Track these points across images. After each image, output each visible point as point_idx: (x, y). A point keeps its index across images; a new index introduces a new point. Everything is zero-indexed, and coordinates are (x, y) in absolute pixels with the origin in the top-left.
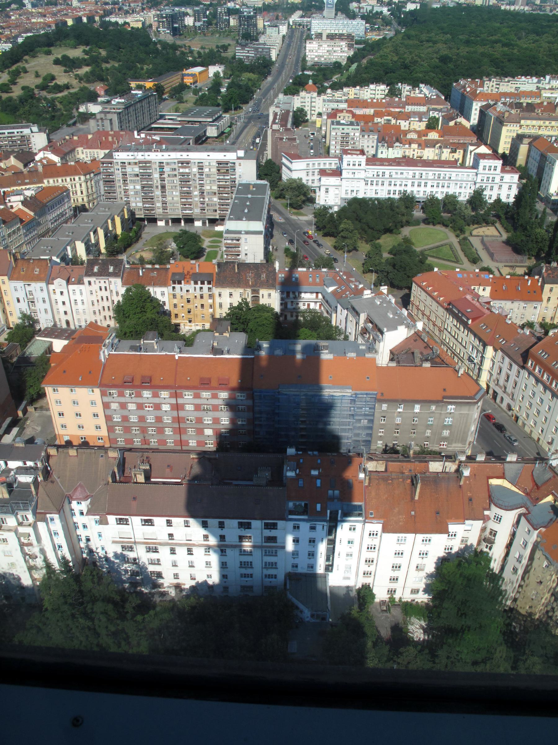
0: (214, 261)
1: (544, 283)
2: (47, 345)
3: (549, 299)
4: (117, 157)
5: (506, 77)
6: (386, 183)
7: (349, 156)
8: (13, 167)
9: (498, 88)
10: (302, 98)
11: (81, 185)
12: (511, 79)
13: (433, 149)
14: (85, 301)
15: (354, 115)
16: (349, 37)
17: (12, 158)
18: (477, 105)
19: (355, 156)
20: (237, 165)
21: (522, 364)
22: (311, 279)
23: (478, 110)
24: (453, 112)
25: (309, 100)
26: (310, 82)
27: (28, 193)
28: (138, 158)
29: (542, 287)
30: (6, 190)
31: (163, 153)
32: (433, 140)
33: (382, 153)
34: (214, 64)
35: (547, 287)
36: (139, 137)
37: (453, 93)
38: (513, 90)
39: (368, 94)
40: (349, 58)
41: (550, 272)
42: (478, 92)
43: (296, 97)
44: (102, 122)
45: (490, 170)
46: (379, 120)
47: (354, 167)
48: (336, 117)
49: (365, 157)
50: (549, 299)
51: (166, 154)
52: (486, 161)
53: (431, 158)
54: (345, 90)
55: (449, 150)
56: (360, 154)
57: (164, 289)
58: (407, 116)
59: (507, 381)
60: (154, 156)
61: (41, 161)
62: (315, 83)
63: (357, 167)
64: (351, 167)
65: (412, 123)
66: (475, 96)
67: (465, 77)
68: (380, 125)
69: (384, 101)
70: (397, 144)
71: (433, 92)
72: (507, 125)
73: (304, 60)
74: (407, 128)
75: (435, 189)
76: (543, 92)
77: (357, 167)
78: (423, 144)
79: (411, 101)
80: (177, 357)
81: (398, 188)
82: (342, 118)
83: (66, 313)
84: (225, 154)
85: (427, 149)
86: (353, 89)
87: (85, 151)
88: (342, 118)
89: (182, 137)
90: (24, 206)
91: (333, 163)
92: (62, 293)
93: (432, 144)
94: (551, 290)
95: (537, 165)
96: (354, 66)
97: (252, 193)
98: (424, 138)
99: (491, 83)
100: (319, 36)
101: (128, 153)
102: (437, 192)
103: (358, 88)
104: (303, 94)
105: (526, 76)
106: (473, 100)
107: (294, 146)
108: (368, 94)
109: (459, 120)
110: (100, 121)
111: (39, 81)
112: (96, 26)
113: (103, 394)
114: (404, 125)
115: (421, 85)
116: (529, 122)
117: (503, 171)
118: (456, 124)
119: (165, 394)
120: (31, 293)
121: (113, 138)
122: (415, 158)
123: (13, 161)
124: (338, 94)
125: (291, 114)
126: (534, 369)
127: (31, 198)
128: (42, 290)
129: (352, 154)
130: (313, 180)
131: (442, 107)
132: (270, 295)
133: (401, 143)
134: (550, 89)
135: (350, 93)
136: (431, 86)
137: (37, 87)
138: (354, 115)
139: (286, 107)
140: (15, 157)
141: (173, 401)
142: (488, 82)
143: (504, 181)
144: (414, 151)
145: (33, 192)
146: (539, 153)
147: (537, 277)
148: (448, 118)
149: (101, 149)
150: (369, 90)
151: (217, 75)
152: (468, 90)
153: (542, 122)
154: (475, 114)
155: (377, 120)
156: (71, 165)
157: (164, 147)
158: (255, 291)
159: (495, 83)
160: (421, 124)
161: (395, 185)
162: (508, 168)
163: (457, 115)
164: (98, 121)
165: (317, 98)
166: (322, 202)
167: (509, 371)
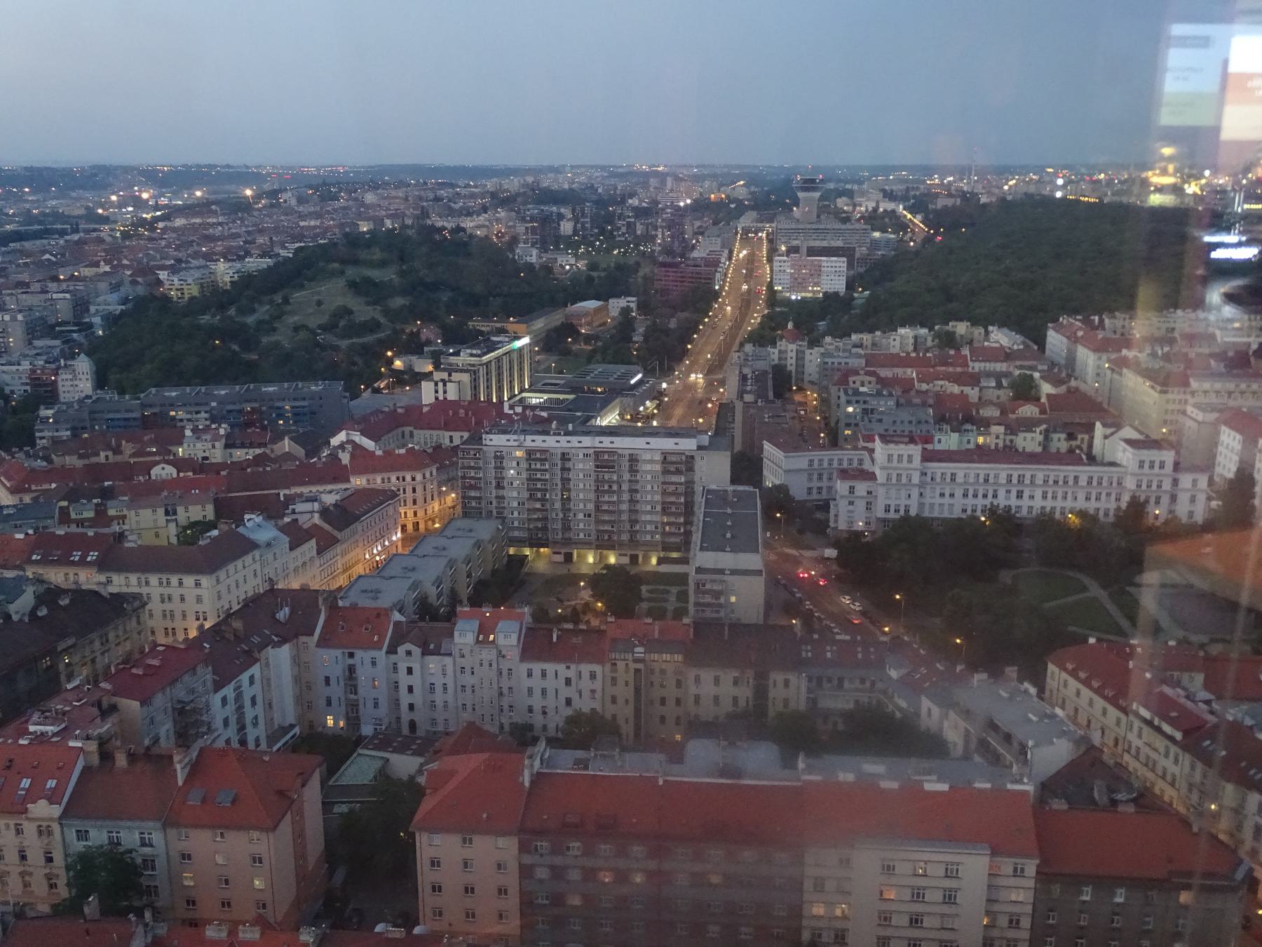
0: (686, 620)
2: (379, 764)
4: (488, 443)
6: (959, 493)
8: (288, 456)
11: (414, 490)
14: (448, 686)
17: (287, 440)
19: (902, 446)
20: (697, 458)
22: (860, 656)
25: (794, 354)
27: (330, 499)
28: (526, 444)
30: (287, 492)
31: (569, 438)
34: (618, 295)
36: (511, 412)
44: (445, 385)
45: (1152, 467)
46: (924, 387)
51: (574, 439)
54: (854, 337)
55: (1063, 436)
57: (597, 668)
60: (550, 442)
61: (342, 446)
68: (931, 394)
70: (968, 427)
75: (1049, 504)
80: (661, 782)
81: (980, 502)
82: (858, 383)
83: (411, 707)
84: (676, 440)
85: (1022, 435)
87: (416, 432)
88: (858, 383)
89: (579, 414)
90: (325, 520)
92: (410, 671)
97: (732, 505)
101: (508, 437)
102: (1053, 508)
103: (878, 333)
104: (782, 345)
110: (440, 384)
111: (324, 320)
112: (410, 232)
113: (524, 848)
114: (972, 393)
119: (637, 850)
120: (352, 669)
121: (467, 414)
123: (286, 445)
125: (771, 376)
127: (336, 505)
128: (374, 664)
129: (897, 443)
130: (820, 488)
132: (787, 683)
137: (320, 327)
138: (881, 381)
139: (762, 365)
140: (291, 439)
141: (652, 865)
144: (997, 437)
145: (338, 497)
149: (446, 430)
151: (626, 311)
156: (399, 455)
157: (570, 426)
158: (761, 677)
160: (1001, 392)
161: (975, 496)
164: (436, 384)
165: (808, 352)
166: (842, 526)
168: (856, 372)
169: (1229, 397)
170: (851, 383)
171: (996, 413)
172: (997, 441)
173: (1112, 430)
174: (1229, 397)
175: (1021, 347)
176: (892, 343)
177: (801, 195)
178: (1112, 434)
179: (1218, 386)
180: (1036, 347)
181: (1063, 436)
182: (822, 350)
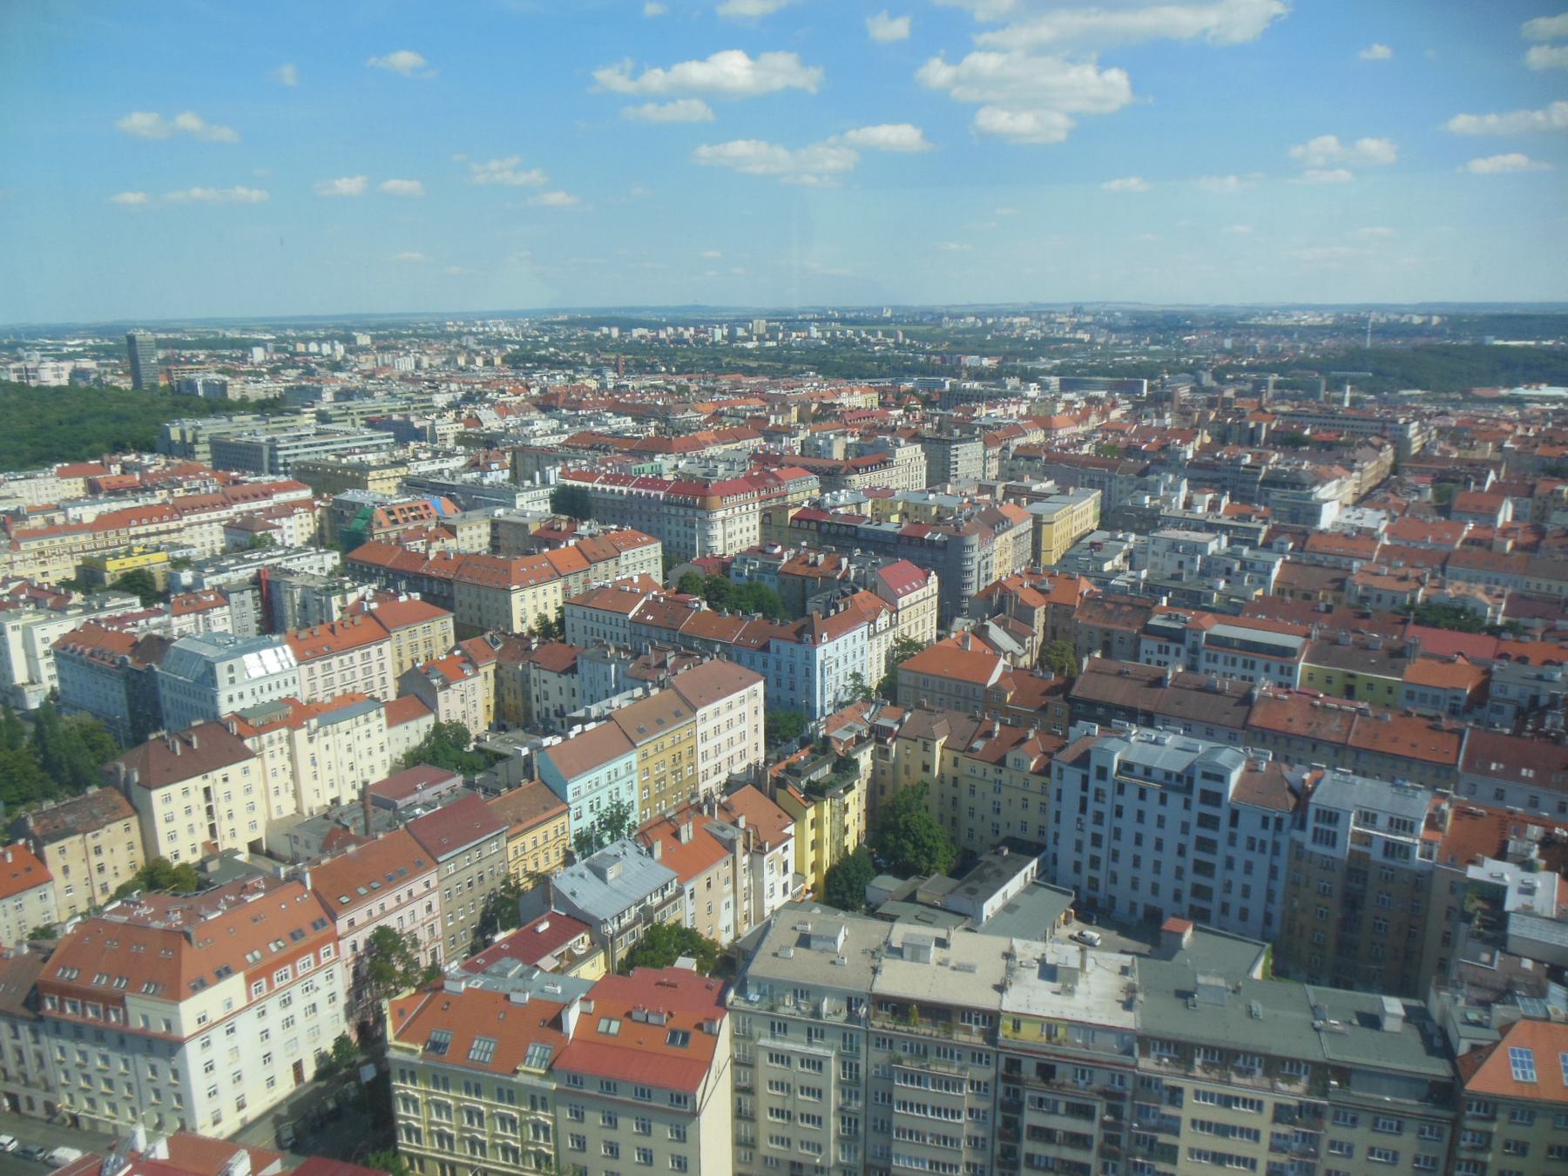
1: (39, 845)
3: (66, 870)
21: (33, 1016)
29: (40, 857)
35: (50, 850)
41: (44, 822)
50: (66, 870)
59: (21, 1061)
94: (62, 851)
126: (62, 1010)
147: (21, 842)
167: (16, 1042)
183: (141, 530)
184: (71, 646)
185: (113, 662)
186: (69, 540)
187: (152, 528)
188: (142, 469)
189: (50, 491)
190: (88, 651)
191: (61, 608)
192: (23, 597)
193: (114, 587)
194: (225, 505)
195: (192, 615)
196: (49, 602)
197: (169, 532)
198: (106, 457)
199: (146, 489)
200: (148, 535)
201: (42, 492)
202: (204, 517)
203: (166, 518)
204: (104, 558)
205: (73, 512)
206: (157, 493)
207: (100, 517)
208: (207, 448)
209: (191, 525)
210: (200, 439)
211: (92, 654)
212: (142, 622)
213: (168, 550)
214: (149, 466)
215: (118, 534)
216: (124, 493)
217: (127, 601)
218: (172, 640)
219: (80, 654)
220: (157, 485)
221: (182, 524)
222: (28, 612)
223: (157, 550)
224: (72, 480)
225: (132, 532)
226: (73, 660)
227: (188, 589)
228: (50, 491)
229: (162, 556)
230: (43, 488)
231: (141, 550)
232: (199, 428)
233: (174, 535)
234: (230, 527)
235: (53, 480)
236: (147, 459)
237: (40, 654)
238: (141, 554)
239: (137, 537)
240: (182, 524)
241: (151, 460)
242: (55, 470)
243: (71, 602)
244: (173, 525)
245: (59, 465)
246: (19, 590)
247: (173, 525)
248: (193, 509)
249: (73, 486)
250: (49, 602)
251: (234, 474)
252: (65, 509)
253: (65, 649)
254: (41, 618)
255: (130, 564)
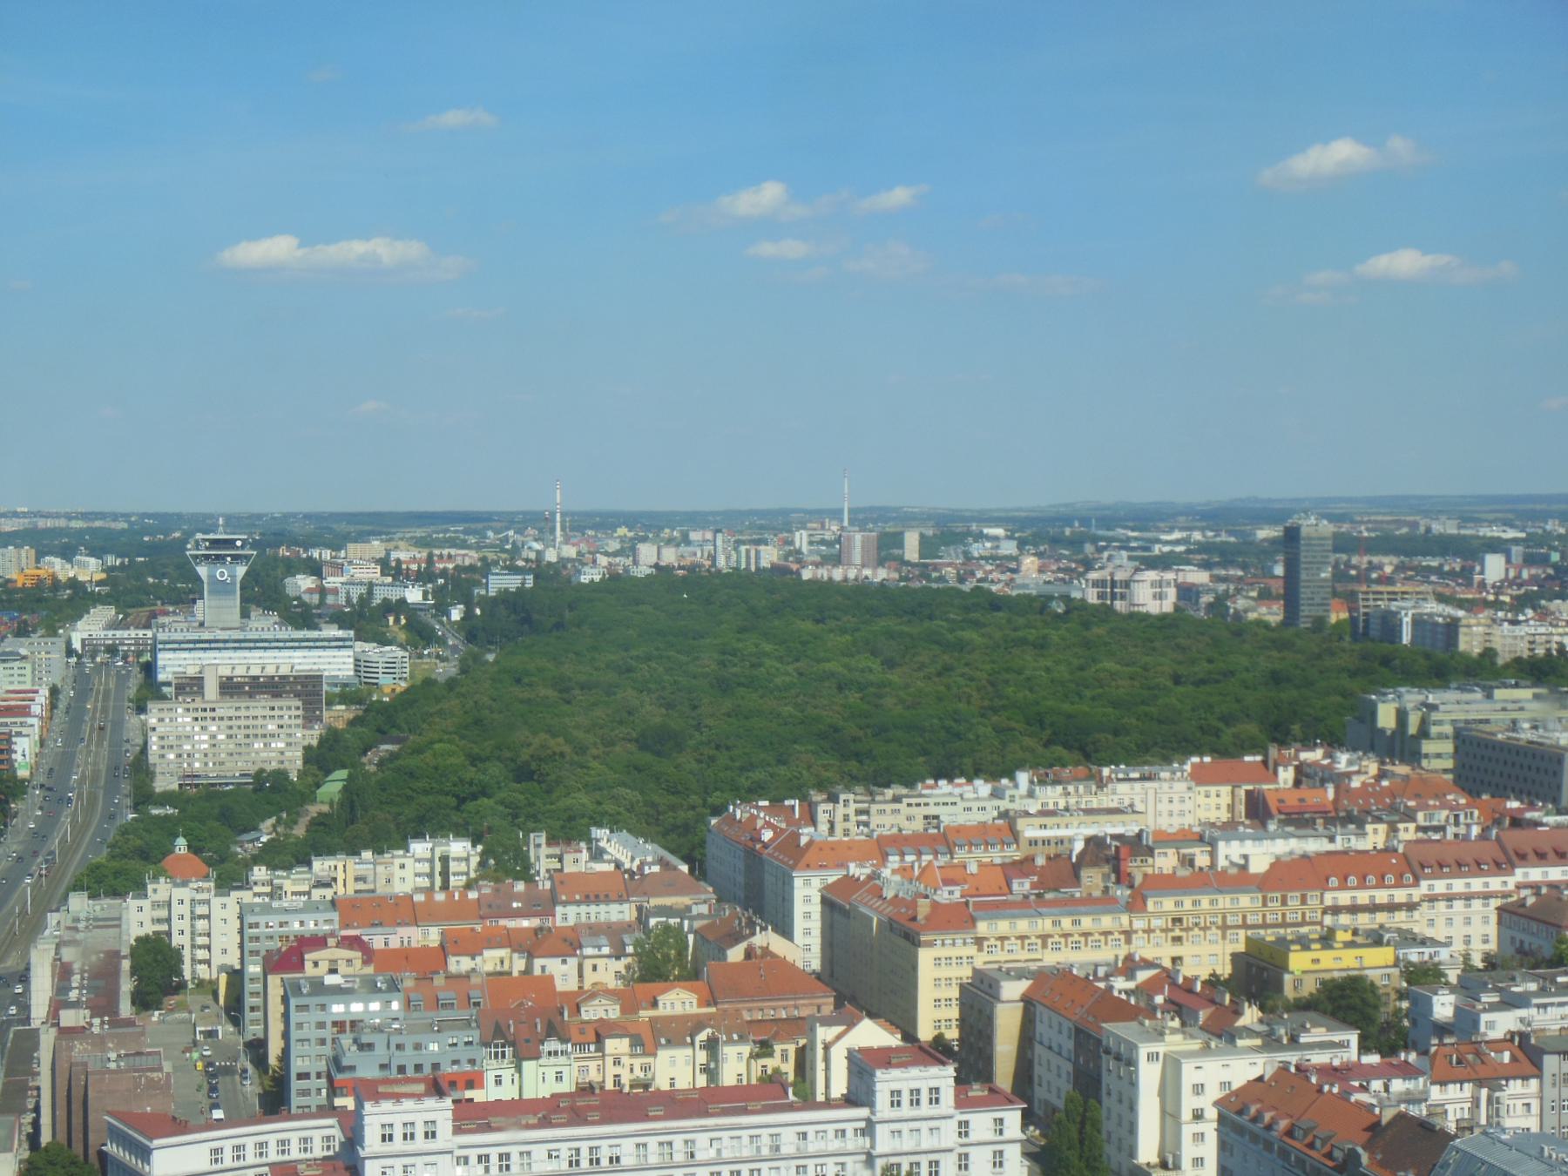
5: (887, 785)
7: (387, 1105)
9: (866, 824)
10: (156, 905)
12: (904, 791)
13: (689, 1051)
15: (369, 954)
16: (307, 689)
18: (807, 883)
19: (408, 1104)
23: (817, 899)
24: (734, 916)
25: (185, 909)
26: (181, 842)
32: (684, 1018)
33: (498, 1081)
37: (711, 850)
38: (918, 825)
39: (408, 873)
40: (310, 755)
42: (804, 840)
43: (132, 903)
47: (410, 1147)
48: (300, 966)
49: (448, 1102)
52: (895, 1073)
53: (683, 1083)
54: (320, 866)
55: (746, 1049)
56: (427, 1094)
58: (569, 944)
62: (194, 849)
63: (420, 1143)
64: (398, 1144)
65: (588, 964)
66: (795, 854)
67: (751, 793)
69: (473, 895)
70: (552, 1045)
71: (646, 853)
72: (931, 944)
73: (141, 767)
74: (571, 985)
76: (1021, 824)
77: (420, 1143)
78: (647, 1036)
79: (564, 888)
85: (664, 1055)
86: (351, 861)
91: (317, 1136)
93: (677, 1032)
95: (1069, 1067)
96: (333, 787)
98: (645, 1014)
99: (841, 810)
100: (190, 686)
103: (367, 855)
104: (160, 889)
105: (950, 778)
106: (793, 868)
107: (152, 1084)
108: (408, 873)
109: (759, 940)
114: (562, 973)
115: (600, 833)
116: (1003, 926)
117: (962, 1103)
118: (749, 954)
122: (626, 1089)
124: (294, 882)
125: (126, 965)
129: (397, 1097)
131: (685, 900)
133: (564, 1041)
134: (1044, 813)
135: (340, 876)
136: (635, 832)
138: (369, 954)
139: (103, 939)
142: (829, 806)
143: (973, 1137)
144: (617, 1062)
146: (1067, 1025)
148: (718, 938)
150: (409, 862)
152: (767, 835)
153: (1048, 922)
154: (807, 916)
155: (460, 964)
159: (853, 807)
162: (977, 1090)
163: (751, 924)
165: (217, 902)
168: (319, 942)
169: (1044, 946)
170: (308, 965)
171: (614, 1012)
172: (618, 1070)
173: (841, 1028)
174: (1044, 946)
175: (656, 869)
176: (398, 873)
177: (202, 571)
178: (839, 1037)
179: (1023, 926)
180: (685, 868)
181: (746, 1049)
182: (246, 896)
183: (1344, 898)
184: (1253, 1110)
185: (1329, 1155)
186: (1224, 901)
187: (1363, 897)
188: (1340, 779)
189: (1176, 807)
190: (1283, 1124)
191: (1223, 1032)
192: (1159, 999)
193: (1305, 1006)
194: (1503, 865)
195: (1468, 1087)
196: (1203, 1015)
197: (1392, 907)
198: (1273, 751)
199: (1349, 819)
200: (1354, 909)
201: (1164, 807)
202: (1458, 885)
203: (1390, 879)
204: (1283, 945)
205: (1230, 852)
206: (1369, 828)
207: (1277, 864)
208: (1448, 747)
209: (1432, 899)
210: (1434, 730)
211: (1290, 1133)
212: (1377, 1085)
213: (1397, 946)
214: (1348, 775)
215: (1304, 901)
216: (1310, 823)
217: (1337, 1037)
218: (1447, 1137)
219: (1269, 1127)
220: (1368, 813)
221: (1417, 893)
222: (1174, 1031)
223: (1376, 938)
224: (1213, 789)
225: (1329, 899)
226: (1255, 1138)
227: (1442, 1029)
228: (1176, 807)
229: (1384, 955)
230: (1165, 798)
231: (1348, 937)
232: (1433, 708)
233: (1401, 916)
234: (1510, 914)
235: (1181, 787)
236: (1343, 760)
237: (1186, 1115)
238: (1349, 945)
239: (1336, 910)
240: (1417, 893)
241: (1350, 763)
242: (1188, 767)
243: (1241, 1022)
244: (1400, 895)
245: (1196, 759)
246: (1146, 990)
247: (1400, 895)
248: (1441, 867)
249: (1213, 800)
250: (1203, 1015)
251: (1514, 804)
252: (1212, 844)
253: (1240, 1112)
254: (1195, 1045)
255: (1338, 962)
